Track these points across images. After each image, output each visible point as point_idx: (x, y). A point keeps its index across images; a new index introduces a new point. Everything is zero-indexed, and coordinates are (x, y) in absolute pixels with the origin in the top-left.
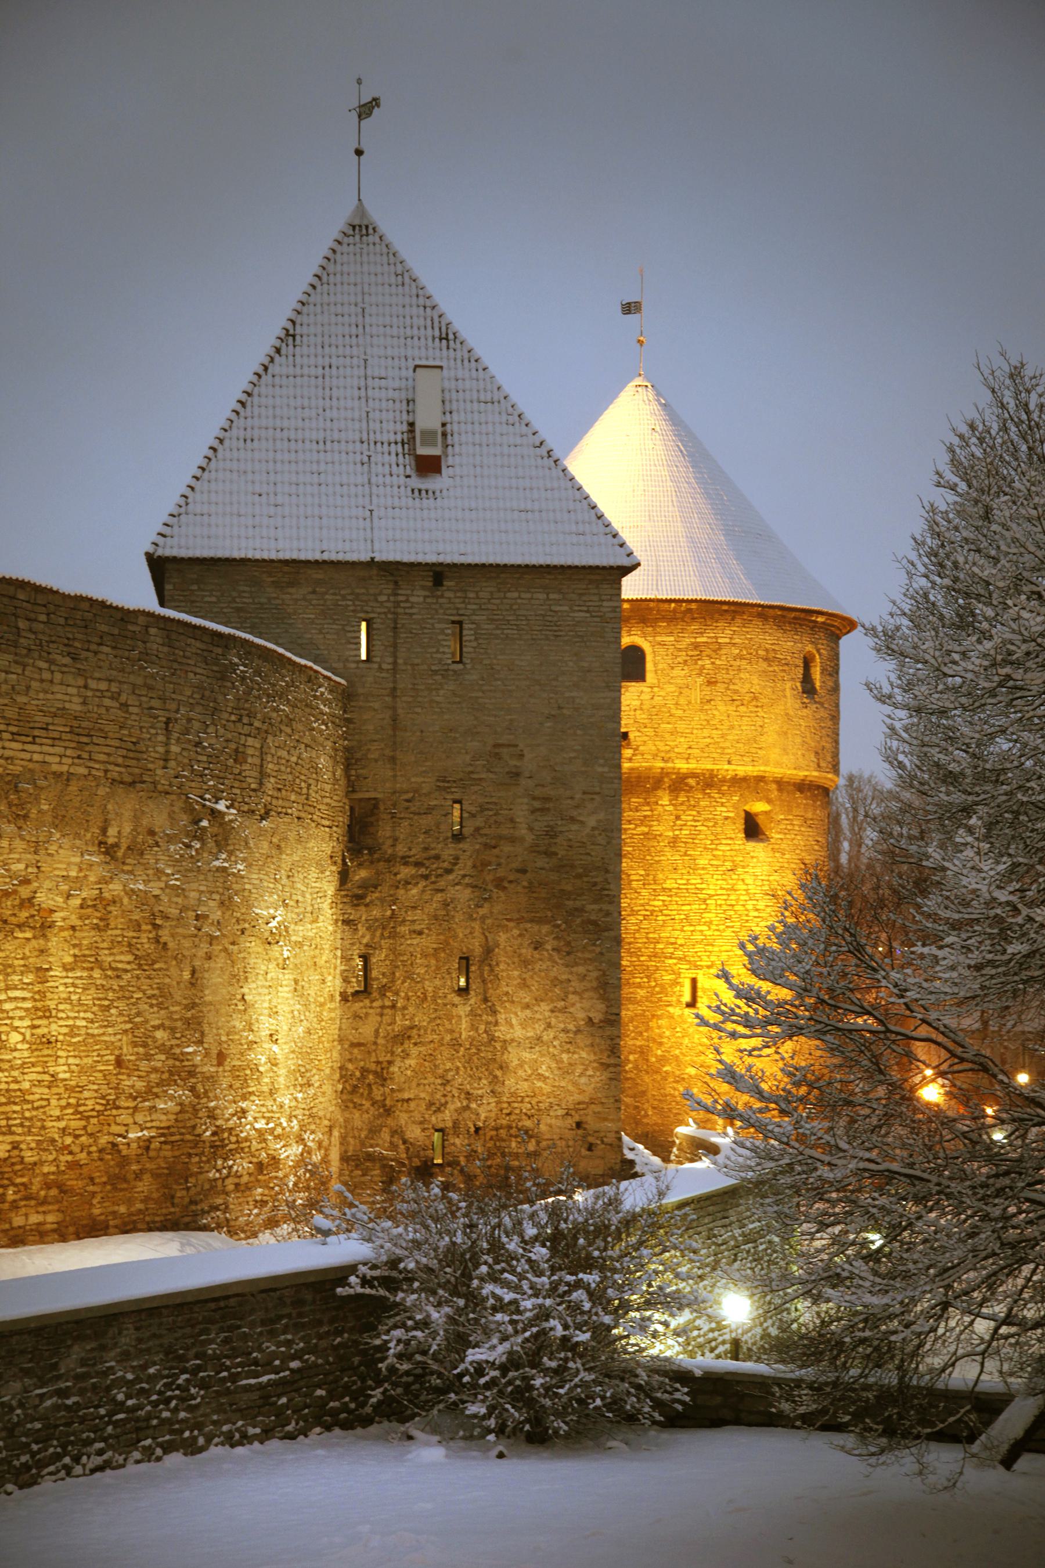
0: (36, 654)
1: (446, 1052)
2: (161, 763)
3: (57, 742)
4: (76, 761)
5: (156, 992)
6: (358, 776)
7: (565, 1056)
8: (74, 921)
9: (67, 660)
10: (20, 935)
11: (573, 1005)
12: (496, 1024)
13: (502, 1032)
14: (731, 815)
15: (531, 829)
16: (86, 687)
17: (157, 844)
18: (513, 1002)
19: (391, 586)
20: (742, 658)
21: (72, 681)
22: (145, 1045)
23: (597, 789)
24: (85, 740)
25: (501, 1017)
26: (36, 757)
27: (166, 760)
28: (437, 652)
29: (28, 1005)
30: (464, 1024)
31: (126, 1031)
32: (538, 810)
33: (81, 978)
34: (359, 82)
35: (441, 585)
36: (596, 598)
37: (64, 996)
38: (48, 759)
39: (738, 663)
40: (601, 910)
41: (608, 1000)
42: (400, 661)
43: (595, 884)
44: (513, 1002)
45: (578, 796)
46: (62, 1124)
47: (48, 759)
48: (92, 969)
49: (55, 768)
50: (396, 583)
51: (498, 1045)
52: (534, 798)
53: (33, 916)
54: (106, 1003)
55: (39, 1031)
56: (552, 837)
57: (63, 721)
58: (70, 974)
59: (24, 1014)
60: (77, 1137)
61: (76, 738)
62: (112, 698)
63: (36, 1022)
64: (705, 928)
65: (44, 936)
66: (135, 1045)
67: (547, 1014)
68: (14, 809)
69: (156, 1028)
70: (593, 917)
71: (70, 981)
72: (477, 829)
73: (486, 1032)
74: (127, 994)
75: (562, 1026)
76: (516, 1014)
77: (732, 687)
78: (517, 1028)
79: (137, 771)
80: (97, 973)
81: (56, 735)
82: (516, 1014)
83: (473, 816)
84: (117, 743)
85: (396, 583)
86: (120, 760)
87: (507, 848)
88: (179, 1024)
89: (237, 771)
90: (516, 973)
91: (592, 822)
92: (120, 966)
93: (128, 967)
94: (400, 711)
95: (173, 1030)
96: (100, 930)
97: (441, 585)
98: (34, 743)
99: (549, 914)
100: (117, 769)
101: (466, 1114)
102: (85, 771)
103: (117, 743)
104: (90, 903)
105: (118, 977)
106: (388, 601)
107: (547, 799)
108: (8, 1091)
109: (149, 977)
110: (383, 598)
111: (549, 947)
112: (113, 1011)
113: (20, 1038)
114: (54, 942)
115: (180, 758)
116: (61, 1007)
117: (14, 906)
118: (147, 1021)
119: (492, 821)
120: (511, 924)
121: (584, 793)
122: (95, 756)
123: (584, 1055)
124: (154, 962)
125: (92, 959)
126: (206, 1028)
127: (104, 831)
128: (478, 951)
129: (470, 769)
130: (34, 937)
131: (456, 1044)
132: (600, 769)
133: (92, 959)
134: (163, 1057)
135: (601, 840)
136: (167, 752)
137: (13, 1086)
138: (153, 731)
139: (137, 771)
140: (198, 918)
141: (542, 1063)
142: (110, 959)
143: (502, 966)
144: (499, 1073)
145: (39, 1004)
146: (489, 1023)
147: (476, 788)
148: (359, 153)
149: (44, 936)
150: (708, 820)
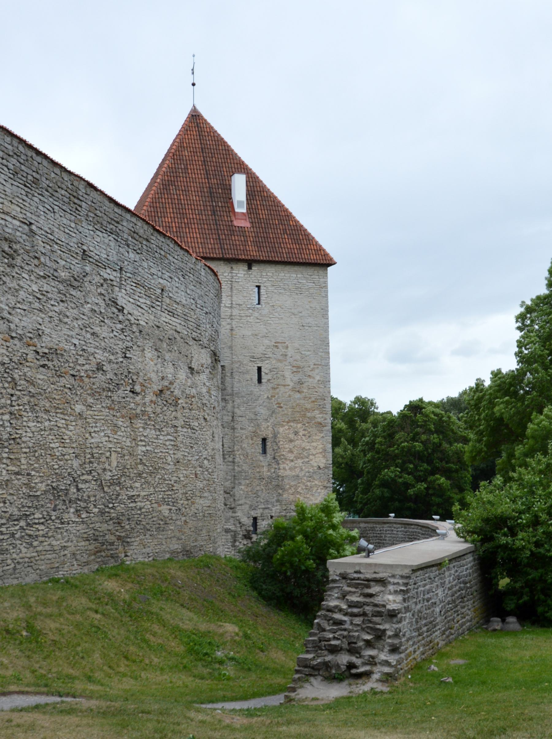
1: (257, 482)
7: (309, 484)
11: (312, 460)
12: (279, 469)
13: (281, 473)
19: (229, 269)
25: (281, 466)
26: (174, 324)
30: (265, 469)
34: (194, 56)
36: (317, 277)
42: (234, 303)
45: (312, 366)
46: (182, 502)
49: (178, 330)
50: (232, 268)
51: (280, 479)
55: (176, 456)
60: (186, 508)
63: (175, 452)
67: (301, 464)
70: (319, 420)
72: (269, 380)
75: (307, 470)
78: (288, 471)
80: (189, 430)
83: (266, 374)
85: (232, 268)
87: (282, 389)
90: (287, 446)
91: (318, 378)
94: (234, 326)
95: (209, 460)
101: (267, 511)
102: (186, 333)
107: (298, 367)
110: (226, 274)
111: (301, 434)
119: (275, 376)
120: (285, 424)
122: (189, 326)
123: (316, 482)
132: (320, 354)
143: (281, 443)
144: (280, 491)
146: (275, 468)
148: (194, 85)
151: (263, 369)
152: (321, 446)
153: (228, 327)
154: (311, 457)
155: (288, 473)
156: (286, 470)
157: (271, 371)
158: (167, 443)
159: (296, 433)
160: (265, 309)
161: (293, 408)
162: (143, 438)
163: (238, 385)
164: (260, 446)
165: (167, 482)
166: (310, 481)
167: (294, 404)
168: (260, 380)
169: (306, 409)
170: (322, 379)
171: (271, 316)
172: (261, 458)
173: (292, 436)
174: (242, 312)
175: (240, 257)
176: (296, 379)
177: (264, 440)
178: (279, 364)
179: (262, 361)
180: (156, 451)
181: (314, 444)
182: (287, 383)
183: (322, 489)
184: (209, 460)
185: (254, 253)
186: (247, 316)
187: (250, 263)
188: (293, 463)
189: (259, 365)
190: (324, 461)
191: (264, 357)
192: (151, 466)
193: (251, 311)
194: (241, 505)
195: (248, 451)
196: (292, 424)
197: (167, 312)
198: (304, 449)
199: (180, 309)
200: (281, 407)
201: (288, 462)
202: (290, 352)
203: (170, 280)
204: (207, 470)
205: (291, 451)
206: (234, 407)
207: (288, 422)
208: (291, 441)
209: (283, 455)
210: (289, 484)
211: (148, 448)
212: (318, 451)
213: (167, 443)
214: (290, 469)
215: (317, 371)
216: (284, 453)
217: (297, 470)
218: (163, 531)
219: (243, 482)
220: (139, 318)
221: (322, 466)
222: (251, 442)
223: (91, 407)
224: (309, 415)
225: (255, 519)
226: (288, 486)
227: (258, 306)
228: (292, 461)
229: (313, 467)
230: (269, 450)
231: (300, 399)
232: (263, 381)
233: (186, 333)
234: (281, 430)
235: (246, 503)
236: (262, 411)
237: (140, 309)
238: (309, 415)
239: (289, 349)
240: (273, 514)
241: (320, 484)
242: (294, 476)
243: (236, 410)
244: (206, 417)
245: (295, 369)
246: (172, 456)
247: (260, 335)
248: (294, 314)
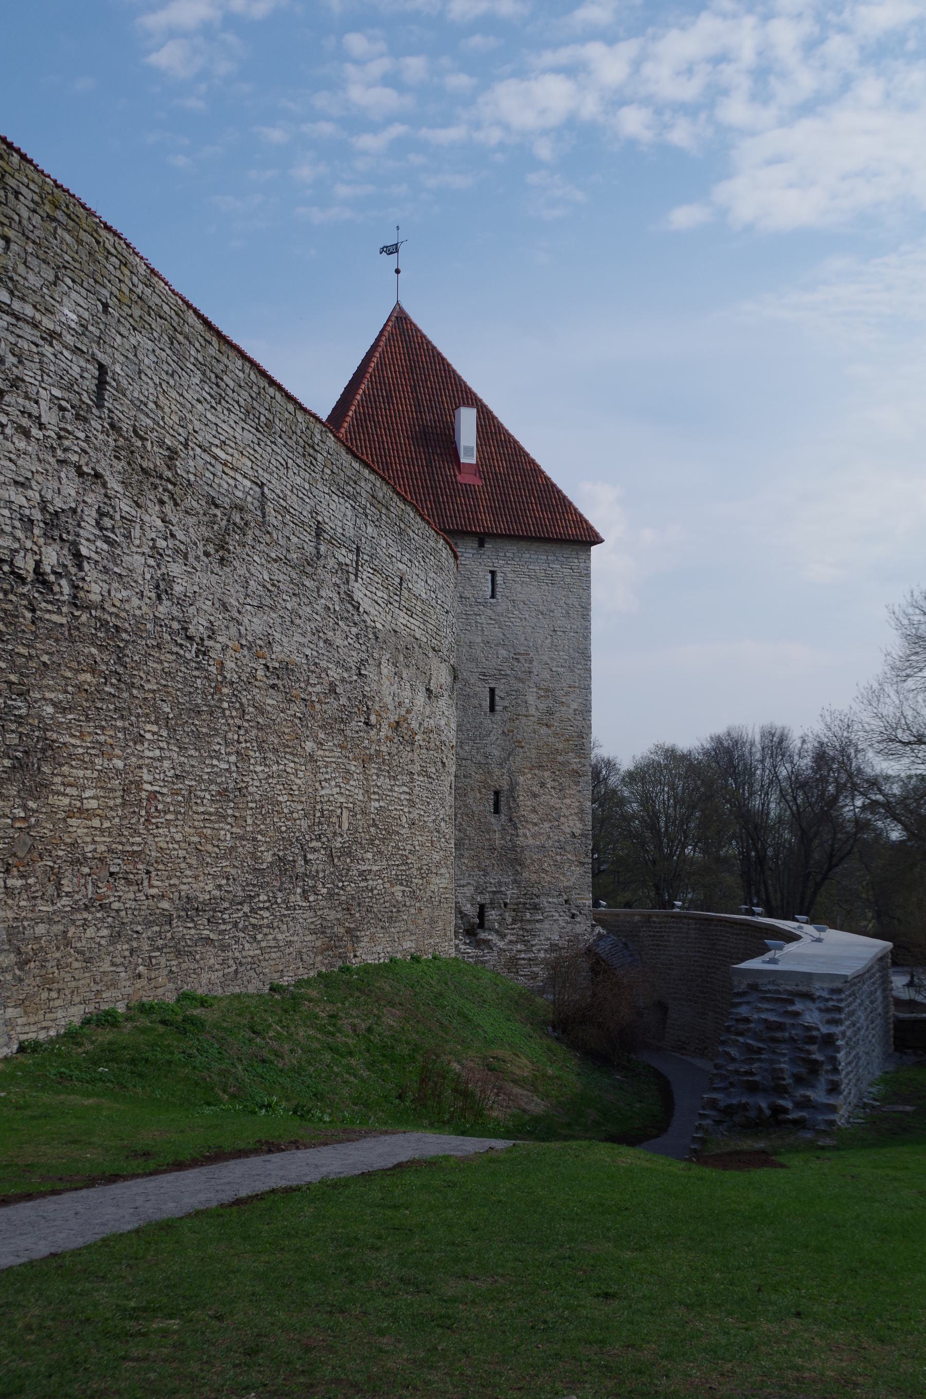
11: (563, 824)
12: (517, 836)
13: (521, 841)
18: (527, 822)
23: (577, 684)
25: (521, 832)
30: (497, 835)
34: (398, 228)
35: (483, 546)
36: (576, 561)
40: (579, 762)
43: (576, 746)
44: (527, 822)
49: (418, 636)
51: (518, 850)
55: (412, 816)
72: (505, 708)
73: (510, 840)
90: (529, 803)
91: (574, 706)
95: (446, 821)
97: (483, 546)
107: (547, 690)
120: (527, 771)
122: (429, 631)
128: (506, 787)
129: (500, 667)
131: (492, 849)
132: (578, 672)
135: (578, 717)
143: (521, 798)
147: (504, 681)
148: (398, 271)
151: (497, 692)
152: (577, 804)
155: (531, 841)
156: (527, 837)
159: (543, 785)
160: (502, 604)
161: (538, 748)
162: (376, 790)
165: (400, 852)
167: (540, 744)
168: (492, 708)
171: (511, 615)
172: (493, 820)
176: (542, 706)
180: (390, 808)
181: (568, 801)
184: (446, 821)
185: (487, 522)
186: (476, 615)
187: (482, 539)
189: (492, 686)
190: (579, 825)
192: (385, 829)
194: (463, 886)
195: (474, 809)
197: (405, 610)
198: (553, 808)
200: (522, 747)
201: (530, 826)
202: (536, 667)
204: (444, 837)
205: (534, 811)
208: (535, 796)
210: (531, 858)
211: (382, 804)
212: (573, 811)
213: (403, 797)
214: (534, 836)
215: (573, 696)
216: (525, 813)
217: (543, 838)
219: (466, 854)
220: (376, 619)
221: (578, 832)
223: (322, 744)
224: (560, 758)
225: (482, 907)
227: (492, 600)
228: (536, 824)
229: (564, 833)
230: (503, 808)
232: (497, 708)
234: (521, 779)
235: (469, 884)
236: (496, 753)
237: (377, 607)
238: (560, 758)
239: (534, 663)
240: (508, 901)
241: (574, 858)
242: (538, 847)
244: (445, 760)
248: (542, 613)
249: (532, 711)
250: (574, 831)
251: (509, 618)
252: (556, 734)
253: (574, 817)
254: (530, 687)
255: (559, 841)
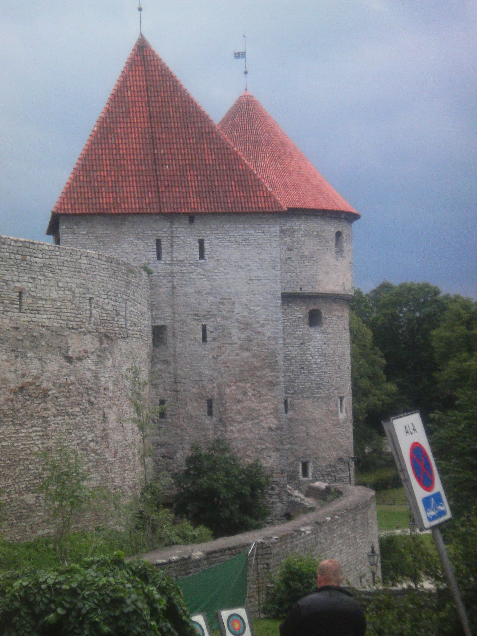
0: (38, 273)
2: (88, 318)
3: (48, 313)
4: (55, 320)
5: (90, 425)
6: (156, 315)
7: (259, 446)
8: (57, 395)
9: (51, 275)
10: (36, 402)
11: (262, 421)
12: (226, 432)
13: (228, 435)
14: (302, 316)
15: (239, 338)
16: (58, 285)
17: (88, 357)
18: (233, 421)
20: (305, 236)
21: (52, 285)
22: (86, 450)
23: (270, 318)
24: (58, 310)
26: (40, 320)
27: (90, 317)
28: (192, 254)
29: (40, 434)
30: (211, 432)
31: (78, 444)
32: (243, 329)
33: (60, 420)
37: (54, 428)
38: (44, 320)
39: (303, 239)
40: (274, 375)
41: (278, 418)
43: (271, 363)
47: (44, 320)
48: (64, 416)
49: (47, 324)
52: (241, 323)
53: (40, 393)
54: (71, 431)
55: (45, 446)
56: (249, 341)
57: (49, 302)
58: (56, 418)
59: (38, 438)
61: (55, 310)
62: (69, 290)
63: (45, 442)
64: (291, 374)
65: (46, 402)
66: (83, 450)
67: (250, 426)
68: (32, 344)
69: (90, 441)
70: (270, 379)
71: (56, 422)
74: (78, 427)
76: (235, 427)
77: (301, 251)
79: (80, 323)
80: (66, 417)
81: (47, 309)
82: (235, 427)
83: (211, 332)
84: (71, 311)
86: (72, 319)
88: (99, 439)
89: (116, 319)
90: (235, 407)
91: (268, 334)
92: (76, 413)
93: (78, 414)
94: (175, 284)
95: (97, 442)
96: (67, 398)
98: (39, 313)
99: (250, 379)
100: (71, 323)
103: (71, 311)
104: (62, 385)
105: (75, 419)
106: (168, 231)
108: (34, 473)
109: (86, 418)
112: (73, 435)
113: (37, 449)
114: (50, 405)
115: (95, 315)
116: (53, 434)
117: (33, 389)
118: (86, 438)
121: (264, 320)
123: (268, 445)
124: (89, 411)
125: (64, 411)
126: (110, 440)
127: (67, 352)
128: (216, 397)
129: (209, 310)
130: (42, 403)
132: (271, 308)
133: (64, 411)
134: (93, 455)
136: (91, 313)
137: (36, 471)
138: (84, 304)
139: (80, 323)
140: (105, 389)
141: (248, 450)
142: (71, 411)
143: (228, 404)
145: (44, 433)
146: (222, 431)
147: (213, 319)
149: (46, 402)
150: (290, 319)
151: (208, 328)
153: (169, 285)
154: (261, 418)
155: (237, 435)
157: (216, 329)
158: (32, 435)
159: (245, 393)
160: (209, 263)
163: (181, 345)
164: (206, 409)
165: (32, 472)
166: (260, 443)
168: (204, 339)
169: (255, 367)
170: (272, 336)
171: (216, 271)
172: (207, 422)
173: (239, 397)
174: (184, 268)
175: (180, 211)
176: (243, 336)
177: (210, 403)
178: (226, 322)
179: (207, 319)
180: (16, 445)
181: (265, 404)
182: (234, 341)
183: (274, 451)
187: (192, 217)
188: (241, 425)
189: (204, 323)
191: (208, 315)
192: (9, 459)
193: (193, 267)
196: (240, 384)
197: (29, 311)
198: (253, 410)
199: (48, 306)
200: (228, 367)
202: (238, 308)
203: (31, 281)
204: (94, 452)
205: (239, 413)
206: (176, 369)
207: (235, 382)
208: (239, 402)
209: (230, 417)
212: (269, 412)
213: (32, 435)
214: (239, 431)
215: (267, 327)
216: (231, 415)
218: (27, 518)
221: (273, 426)
222: (195, 404)
224: (258, 373)
226: (236, 450)
229: (263, 428)
231: (249, 357)
232: (208, 339)
233: (59, 325)
234: (228, 390)
238: (258, 373)
239: (236, 305)
241: (271, 446)
242: (242, 439)
243: (179, 372)
244: (93, 399)
245: (242, 326)
246: (40, 446)
247: (205, 292)
248: (241, 268)
249: (235, 339)
250: (271, 425)
251: (215, 273)
252: (254, 356)
253: (272, 416)
254: (233, 323)
255: (258, 434)
